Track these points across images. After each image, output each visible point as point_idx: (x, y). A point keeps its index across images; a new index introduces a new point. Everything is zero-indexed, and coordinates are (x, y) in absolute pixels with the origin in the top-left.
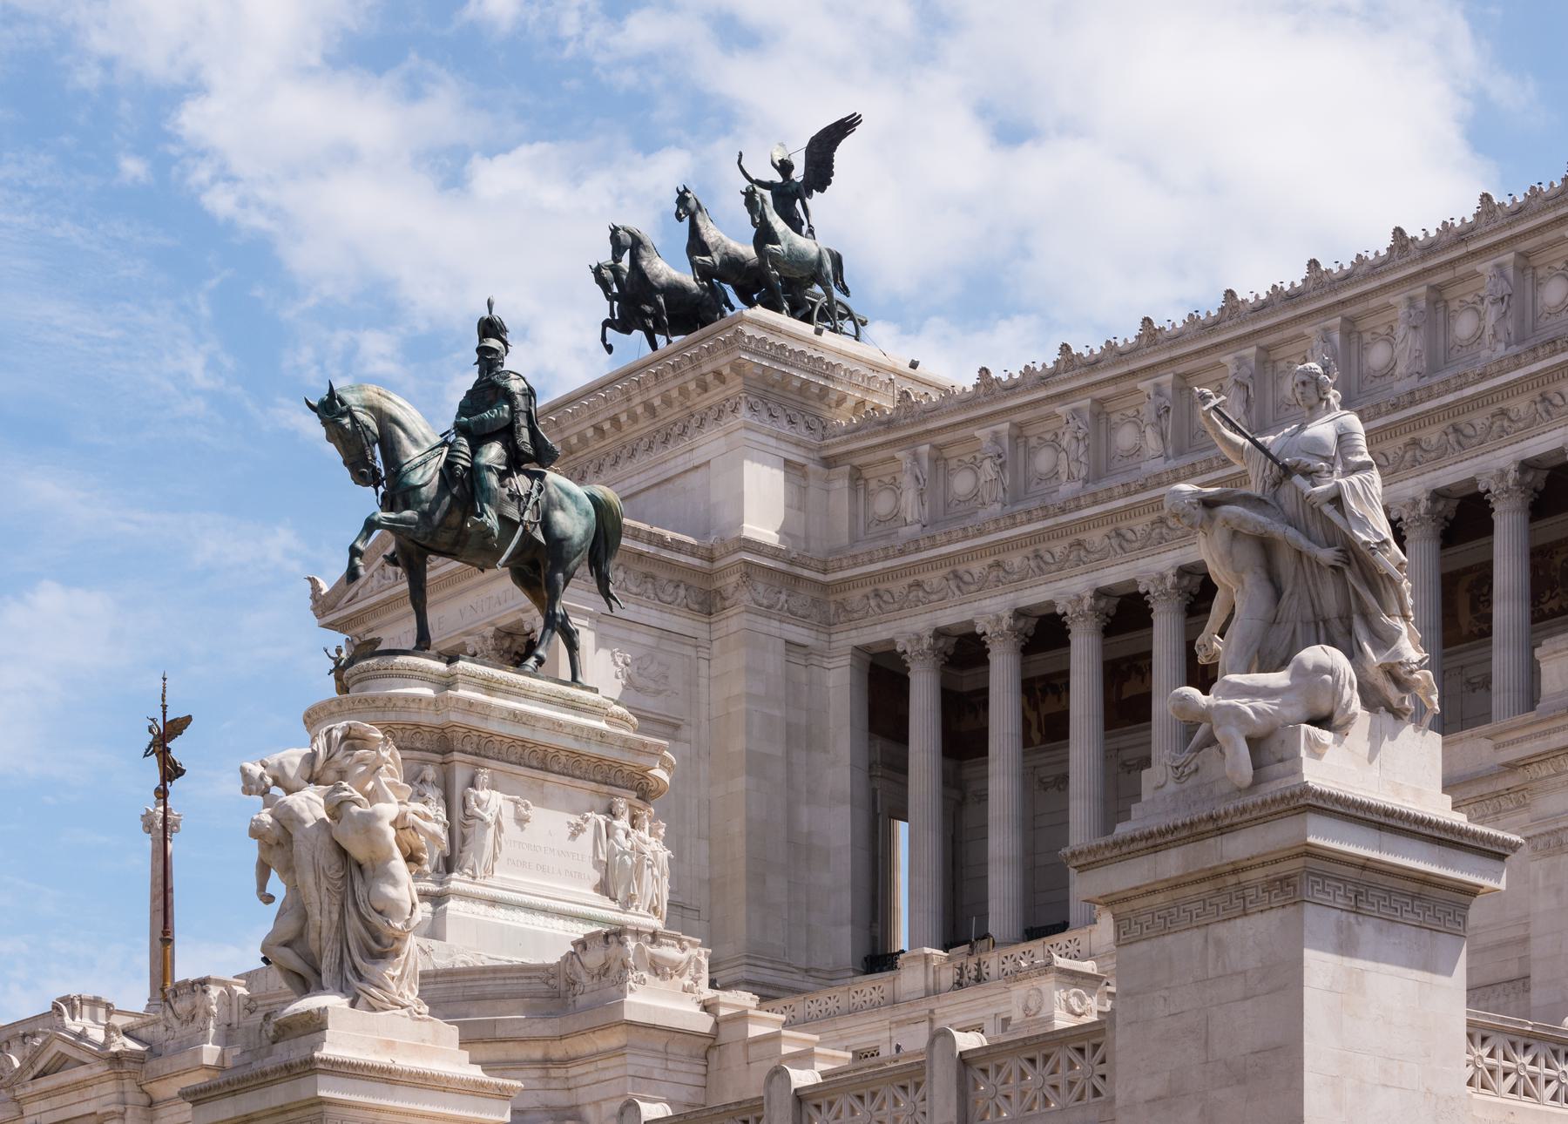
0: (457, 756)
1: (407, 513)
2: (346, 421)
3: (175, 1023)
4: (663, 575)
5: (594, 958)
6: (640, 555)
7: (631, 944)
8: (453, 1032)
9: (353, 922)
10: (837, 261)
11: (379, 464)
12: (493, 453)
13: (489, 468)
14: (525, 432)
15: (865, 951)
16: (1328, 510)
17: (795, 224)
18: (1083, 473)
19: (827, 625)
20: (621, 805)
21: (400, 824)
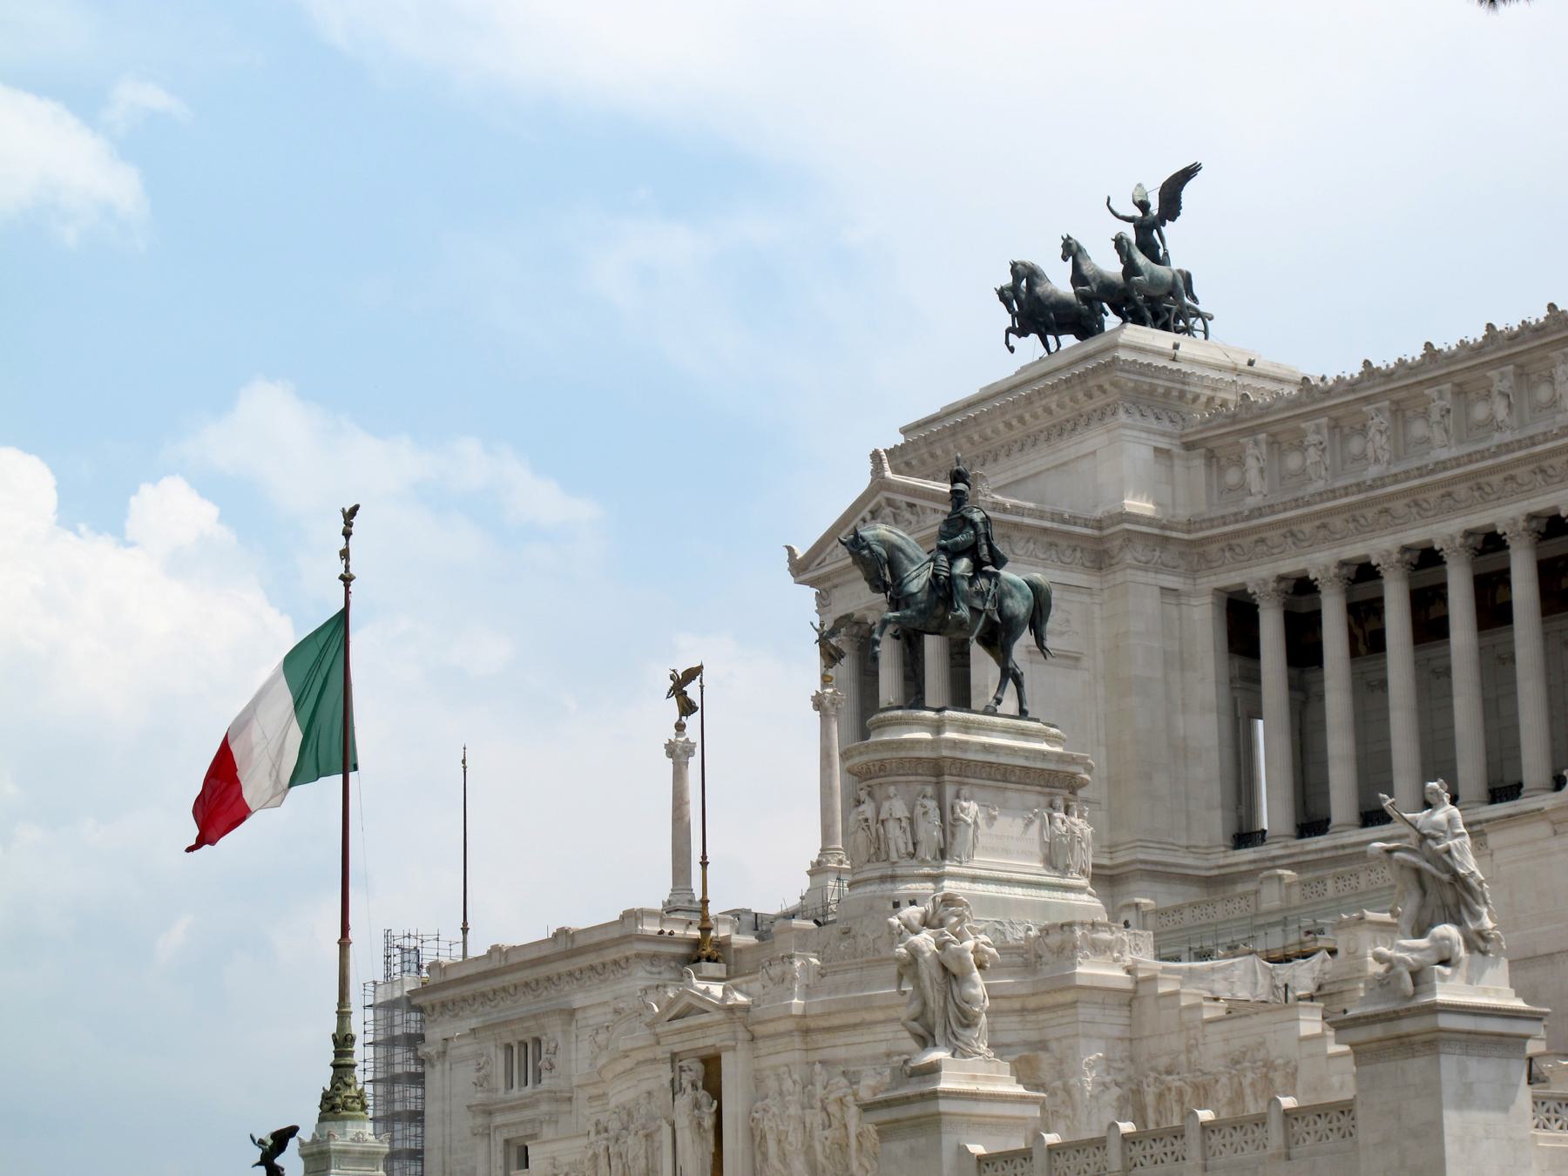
0: (947, 778)
1: (908, 612)
2: (865, 552)
3: (770, 984)
4: (1063, 543)
5: (1054, 939)
6: (1045, 530)
7: (1079, 932)
8: (1006, 1066)
9: (952, 1008)
10: (1188, 278)
11: (888, 579)
12: (963, 565)
13: (963, 577)
14: (985, 547)
15: (1233, 829)
16: (1445, 857)
17: (1156, 259)
18: (1387, 456)
19: (1193, 573)
20: (1059, 802)
21: (976, 951)
